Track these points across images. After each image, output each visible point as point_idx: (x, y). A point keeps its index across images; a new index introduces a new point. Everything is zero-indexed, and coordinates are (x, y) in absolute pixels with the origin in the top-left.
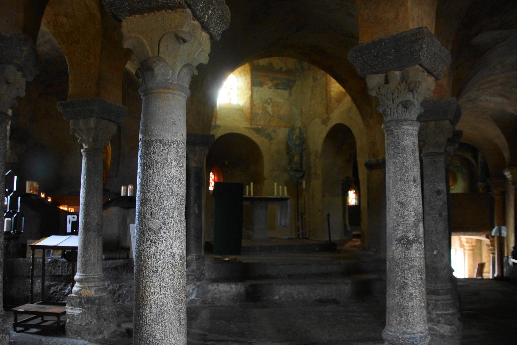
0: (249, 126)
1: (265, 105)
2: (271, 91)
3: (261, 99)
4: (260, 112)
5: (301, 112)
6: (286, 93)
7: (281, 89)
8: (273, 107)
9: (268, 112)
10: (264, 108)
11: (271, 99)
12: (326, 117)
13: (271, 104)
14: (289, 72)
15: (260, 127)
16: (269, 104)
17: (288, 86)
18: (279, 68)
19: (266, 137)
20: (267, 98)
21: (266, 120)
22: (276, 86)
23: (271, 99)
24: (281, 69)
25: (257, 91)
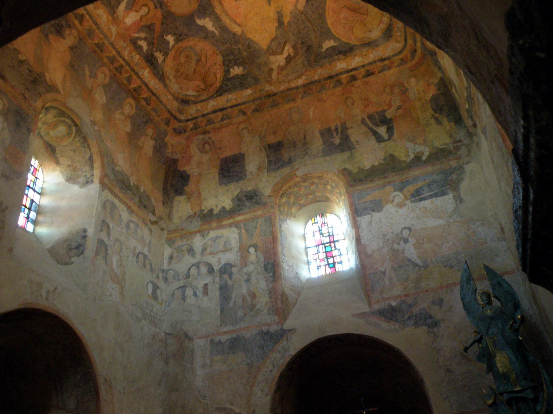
0: (367, 309)
1: (396, 246)
2: (403, 211)
3: (384, 236)
6: (447, 201)
7: (431, 197)
9: (409, 260)
11: (410, 229)
13: (412, 240)
15: (394, 304)
16: (406, 241)
18: (412, 156)
19: (417, 324)
21: (407, 279)
22: (417, 196)
23: (410, 229)
24: (418, 157)
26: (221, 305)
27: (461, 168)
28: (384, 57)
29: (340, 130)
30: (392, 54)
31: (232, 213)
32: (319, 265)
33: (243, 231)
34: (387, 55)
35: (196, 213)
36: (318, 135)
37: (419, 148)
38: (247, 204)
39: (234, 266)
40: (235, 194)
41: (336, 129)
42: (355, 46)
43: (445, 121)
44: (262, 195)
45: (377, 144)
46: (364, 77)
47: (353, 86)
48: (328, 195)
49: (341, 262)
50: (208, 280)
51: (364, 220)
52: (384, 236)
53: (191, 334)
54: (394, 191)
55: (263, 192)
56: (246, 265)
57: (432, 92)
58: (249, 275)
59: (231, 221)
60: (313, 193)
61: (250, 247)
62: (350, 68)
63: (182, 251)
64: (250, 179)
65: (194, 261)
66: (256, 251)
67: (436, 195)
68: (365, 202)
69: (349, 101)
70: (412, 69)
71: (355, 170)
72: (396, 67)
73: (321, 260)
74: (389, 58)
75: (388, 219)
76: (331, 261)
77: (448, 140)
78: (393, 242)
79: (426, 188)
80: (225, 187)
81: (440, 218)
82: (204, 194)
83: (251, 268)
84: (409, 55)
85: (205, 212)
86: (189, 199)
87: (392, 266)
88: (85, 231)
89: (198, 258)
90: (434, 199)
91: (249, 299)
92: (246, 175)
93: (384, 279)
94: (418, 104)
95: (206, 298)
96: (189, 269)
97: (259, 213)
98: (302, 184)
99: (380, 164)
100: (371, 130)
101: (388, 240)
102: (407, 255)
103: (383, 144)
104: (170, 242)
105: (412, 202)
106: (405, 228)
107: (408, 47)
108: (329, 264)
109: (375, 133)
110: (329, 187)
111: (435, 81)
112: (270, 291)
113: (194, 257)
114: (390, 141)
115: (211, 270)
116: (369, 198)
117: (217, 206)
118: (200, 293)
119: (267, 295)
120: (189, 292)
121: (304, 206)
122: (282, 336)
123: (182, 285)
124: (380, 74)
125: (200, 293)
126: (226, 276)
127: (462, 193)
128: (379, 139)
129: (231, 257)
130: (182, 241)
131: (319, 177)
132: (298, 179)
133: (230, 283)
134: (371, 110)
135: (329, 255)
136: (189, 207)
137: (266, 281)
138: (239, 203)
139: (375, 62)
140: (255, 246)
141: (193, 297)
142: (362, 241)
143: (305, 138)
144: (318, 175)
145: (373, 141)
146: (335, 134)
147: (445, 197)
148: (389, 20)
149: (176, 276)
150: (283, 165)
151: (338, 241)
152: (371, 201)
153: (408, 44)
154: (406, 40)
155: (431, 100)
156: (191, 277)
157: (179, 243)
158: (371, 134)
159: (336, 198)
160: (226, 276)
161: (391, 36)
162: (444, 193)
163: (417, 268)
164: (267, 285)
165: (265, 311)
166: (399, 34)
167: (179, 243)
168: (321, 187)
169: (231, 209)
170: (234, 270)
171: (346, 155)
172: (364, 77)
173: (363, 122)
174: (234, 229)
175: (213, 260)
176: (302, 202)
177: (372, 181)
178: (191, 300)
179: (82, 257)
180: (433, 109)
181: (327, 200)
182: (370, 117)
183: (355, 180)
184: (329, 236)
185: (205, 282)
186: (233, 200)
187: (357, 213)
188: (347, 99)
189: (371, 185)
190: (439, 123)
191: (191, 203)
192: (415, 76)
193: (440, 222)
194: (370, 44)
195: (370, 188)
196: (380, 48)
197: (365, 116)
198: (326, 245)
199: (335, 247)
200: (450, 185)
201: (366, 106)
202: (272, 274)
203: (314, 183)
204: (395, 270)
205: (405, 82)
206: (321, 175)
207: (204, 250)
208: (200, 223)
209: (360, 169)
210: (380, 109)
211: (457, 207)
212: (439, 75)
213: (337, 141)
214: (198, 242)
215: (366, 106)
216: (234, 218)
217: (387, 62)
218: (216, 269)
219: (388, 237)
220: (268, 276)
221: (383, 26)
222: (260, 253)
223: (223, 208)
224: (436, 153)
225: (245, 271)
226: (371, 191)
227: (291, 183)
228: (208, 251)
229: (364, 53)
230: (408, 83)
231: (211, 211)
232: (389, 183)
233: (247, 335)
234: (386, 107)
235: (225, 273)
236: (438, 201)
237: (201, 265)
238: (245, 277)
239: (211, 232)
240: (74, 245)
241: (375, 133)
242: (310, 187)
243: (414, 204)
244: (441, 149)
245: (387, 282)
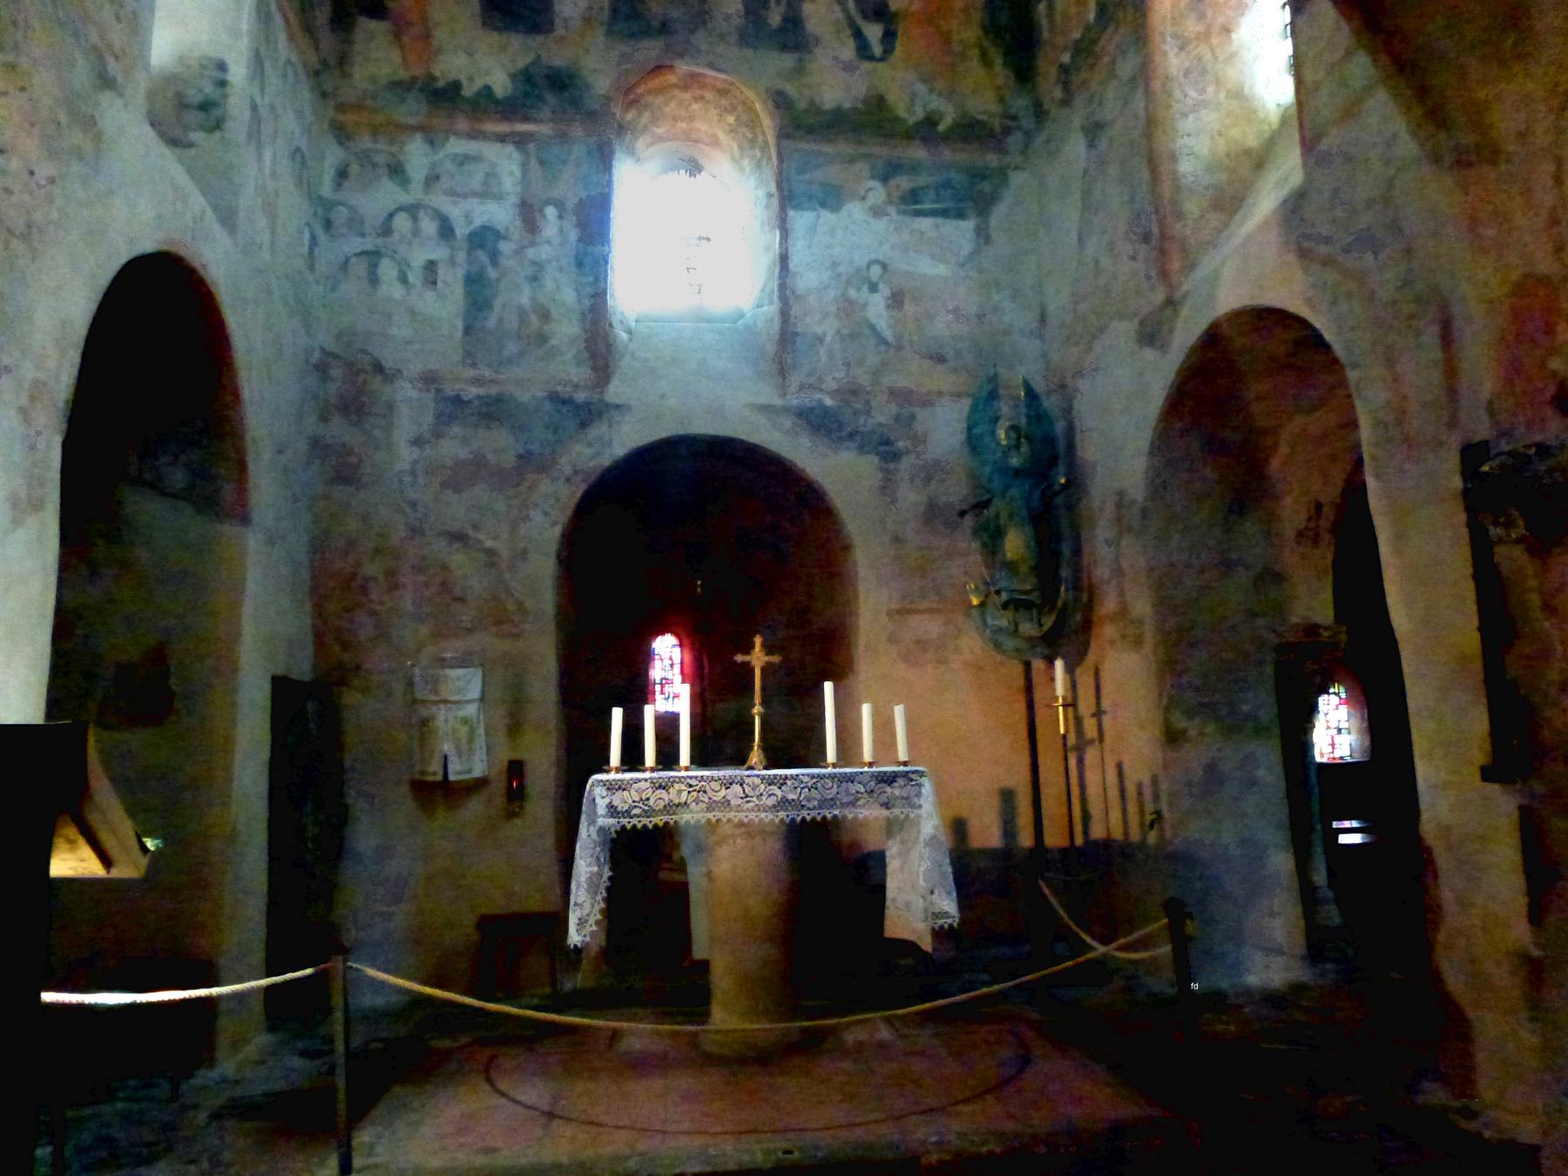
0: (777, 401)
1: (852, 293)
2: (880, 225)
3: (835, 265)
4: (828, 328)
5: (1043, 319)
6: (961, 232)
8: (896, 300)
9: (872, 327)
10: (848, 308)
11: (884, 267)
12: (1159, 296)
13: (885, 290)
16: (873, 288)
17: (972, 198)
18: (920, 114)
19: (861, 449)
20: (861, 259)
22: (911, 202)
23: (884, 267)
24: (930, 121)
25: (812, 230)
26: (465, 320)
27: (1002, 175)
31: (510, 109)
33: (533, 162)
35: (414, 79)
37: (937, 103)
38: (551, 99)
39: (504, 238)
40: (522, 63)
43: (999, 61)
44: (588, 87)
50: (439, 253)
51: (800, 220)
52: (835, 265)
53: (388, 363)
55: (590, 80)
56: (533, 244)
58: (539, 266)
59: (503, 127)
61: (548, 202)
63: (375, 166)
64: (563, 38)
65: (404, 198)
67: (944, 213)
71: (802, 105)
77: (994, 107)
79: (931, 194)
80: (495, 38)
82: (440, 35)
83: (543, 252)
85: (441, 84)
86: (397, 35)
88: (222, 66)
89: (415, 193)
90: (939, 220)
91: (534, 319)
92: (551, 23)
95: (430, 295)
96: (391, 216)
99: (854, 109)
101: (840, 275)
104: (342, 134)
105: (899, 212)
106: (877, 262)
109: (858, 35)
113: (407, 191)
115: (446, 231)
116: (818, 175)
117: (471, 79)
118: (415, 277)
120: (387, 269)
123: (370, 247)
125: (415, 277)
126: (482, 256)
129: (501, 214)
130: (376, 141)
131: (718, 91)
133: (492, 273)
136: (396, 56)
138: (528, 88)
140: (559, 205)
141: (396, 284)
149: (356, 224)
152: (822, 185)
156: (396, 236)
157: (365, 142)
158: (849, 32)
160: (482, 256)
162: (961, 215)
165: (569, 356)
167: (365, 142)
169: (508, 98)
170: (504, 247)
171: (788, 60)
175: (456, 212)
177: (831, 141)
178: (390, 288)
179: (218, 135)
183: (798, 127)
185: (432, 257)
186: (513, 77)
189: (827, 149)
190: (986, 60)
191: (402, 47)
203: (702, 98)
204: (842, 339)
207: (432, 179)
208: (424, 107)
209: (812, 102)
211: (976, 252)
214: (416, 155)
218: (461, 231)
219: (841, 269)
223: (488, 88)
228: (445, 183)
231: (456, 86)
232: (866, 156)
233: (524, 397)
235: (482, 246)
237: (421, 214)
238: (529, 271)
239: (452, 139)
240: (194, 97)
241: (858, 35)
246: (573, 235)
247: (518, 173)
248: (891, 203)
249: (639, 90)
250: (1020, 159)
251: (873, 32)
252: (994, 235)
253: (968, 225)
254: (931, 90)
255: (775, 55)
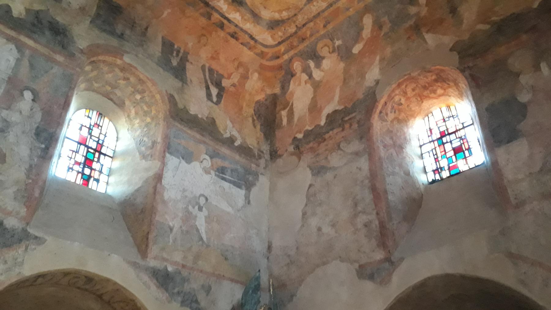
2: (207, 178)
3: (184, 190)
4: (176, 224)
5: (269, 248)
7: (230, 182)
8: (208, 219)
9: (198, 230)
10: (188, 217)
11: (207, 199)
12: (379, 255)
13: (205, 212)
14: (244, 150)
15: (170, 269)
17: (245, 181)
21: (190, 249)
22: (221, 172)
23: (207, 199)
25: (177, 168)
28: (254, 36)
29: (181, 55)
30: (261, 41)
32: (71, 166)
34: (257, 38)
36: (160, 39)
37: (235, 133)
38: (47, 33)
41: (178, 52)
42: (246, 4)
45: (205, 99)
46: (229, 34)
47: (216, 31)
48: (127, 103)
49: (97, 181)
51: (172, 161)
54: (206, 154)
55: (75, 38)
57: (260, 97)
59: (13, 33)
60: (114, 87)
61: (27, 88)
62: (227, 15)
66: (33, 100)
68: (179, 144)
69: (203, 40)
70: (262, 67)
71: (180, 106)
72: (255, 53)
73: (77, 163)
74: (256, 41)
75: (192, 176)
76: (87, 171)
77: (256, 145)
78: (190, 202)
81: (231, 206)
84: (270, 55)
87: (181, 227)
90: (232, 186)
93: (169, 237)
94: (247, 97)
97: (60, 58)
98: (117, 70)
99: (202, 119)
100: (206, 82)
101: (186, 197)
102: (197, 223)
103: (210, 103)
105: (216, 175)
107: (276, 49)
108: (83, 174)
109: (208, 88)
110: (138, 97)
111: (269, 91)
112: (31, 166)
114: (216, 106)
119: (23, 169)
121: (94, 91)
122: (20, 241)
124: (241, 46)
127: (251, 196)
128: (209, 96)
131: (140, 80)
132: (119, 62)
134: (215, 66)
135: (88, 163)
137: (31, 149)
138: (36, 22)
139: (246, 32)
142: (163, 181)
143: (146, 29)
144: (141, 76)
145: (202, 93)
146: (175, 53)
147: (239, 189)
148: (287, 17)
150: (112, 33)
151: (105, 155)
152: (184, 147)
153: (279, 48)
154: (280, 43)
155: (257, 102)
159: (133, 112)
161: (272, 28)
162: (239, 187)
163: (201, 242)
164: (30, 157)
166: (280, 34)
168: (130, 89)
169: (19, 19)
172: (229, 34)
173: (203, 68)
174: (13, 47)
176: (96, 85)
177: (190, 128)
180: (254, 110)
181: (121, 105)
182: (211, 70)
184: (98, 142)
186: (28, 11)
187: (168, 149)
188: (203, 35)
189: (189, 131)
192: (260, 74)
193: (229, 210)
194: (256, 17)
195: (187, 133)
196: (258, 26)
197: (207, 65)
198: (90, 150)
199: (99, 158)
200: (246, 183)
201: (213, 58)
202: (43, 146)
203: (128, 79)
205: (251, 71)
206: (145, 79)
209: (185, 107)
210: (221, 72)
211: (244, 207)
212: (277, 90)
213: (175, 62)
215: (213, 58)
216: (20, 33)
217: (252, 42)
219: (186, 194)
220: (37, 144)
221: (277, 16)
222: (39, 109)
224: (245, 148)
225: (3, 115)
226: (187, 138)
227: (109, 59)
229: (246, 17)
230: (252, 74)
232: (205, 143)
234: (226, 75)
236: (235, 190)
241: (208, 88)
242: (119, 79)
243: (216, 178)
244: (249, 148)
245: (171, 241)
246: (38, 116)
247: (12, 62)
248: (213, 169)
249: (100, 58)
250: (262, 171)
251: (214, 91)
252: (252, 202)
253: (243, 192)
254: (233, 127)
255: (172, 77)
